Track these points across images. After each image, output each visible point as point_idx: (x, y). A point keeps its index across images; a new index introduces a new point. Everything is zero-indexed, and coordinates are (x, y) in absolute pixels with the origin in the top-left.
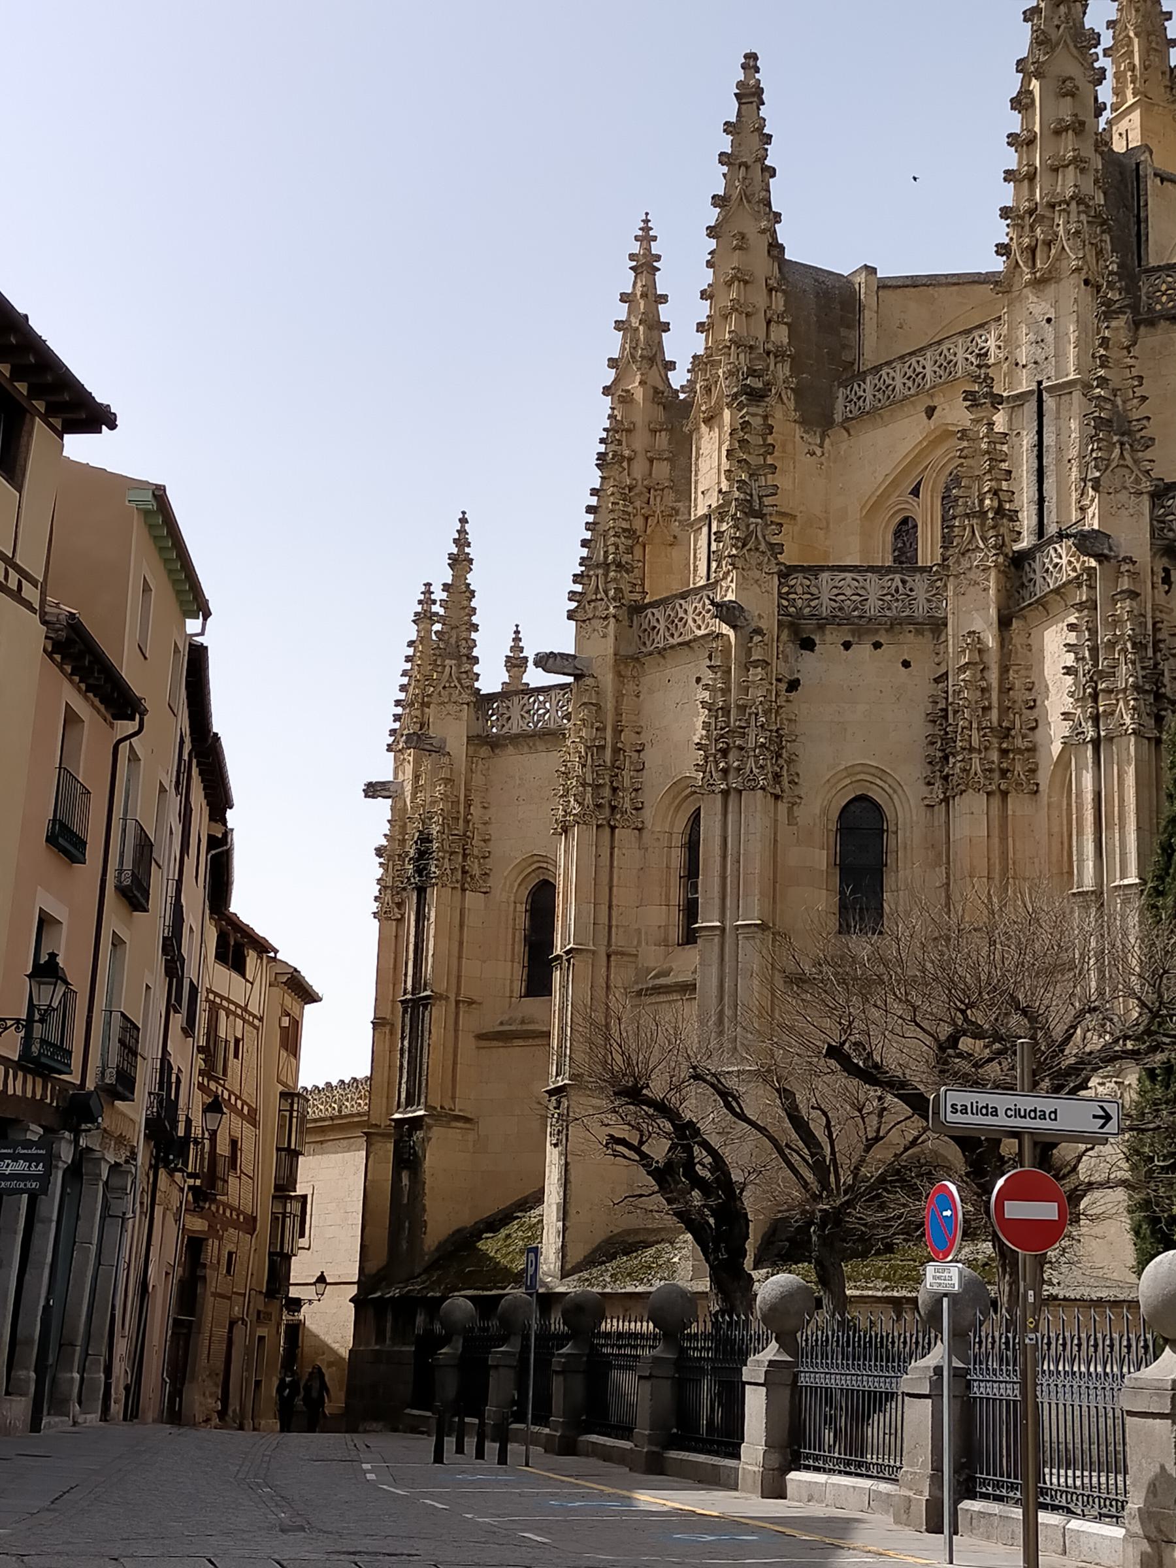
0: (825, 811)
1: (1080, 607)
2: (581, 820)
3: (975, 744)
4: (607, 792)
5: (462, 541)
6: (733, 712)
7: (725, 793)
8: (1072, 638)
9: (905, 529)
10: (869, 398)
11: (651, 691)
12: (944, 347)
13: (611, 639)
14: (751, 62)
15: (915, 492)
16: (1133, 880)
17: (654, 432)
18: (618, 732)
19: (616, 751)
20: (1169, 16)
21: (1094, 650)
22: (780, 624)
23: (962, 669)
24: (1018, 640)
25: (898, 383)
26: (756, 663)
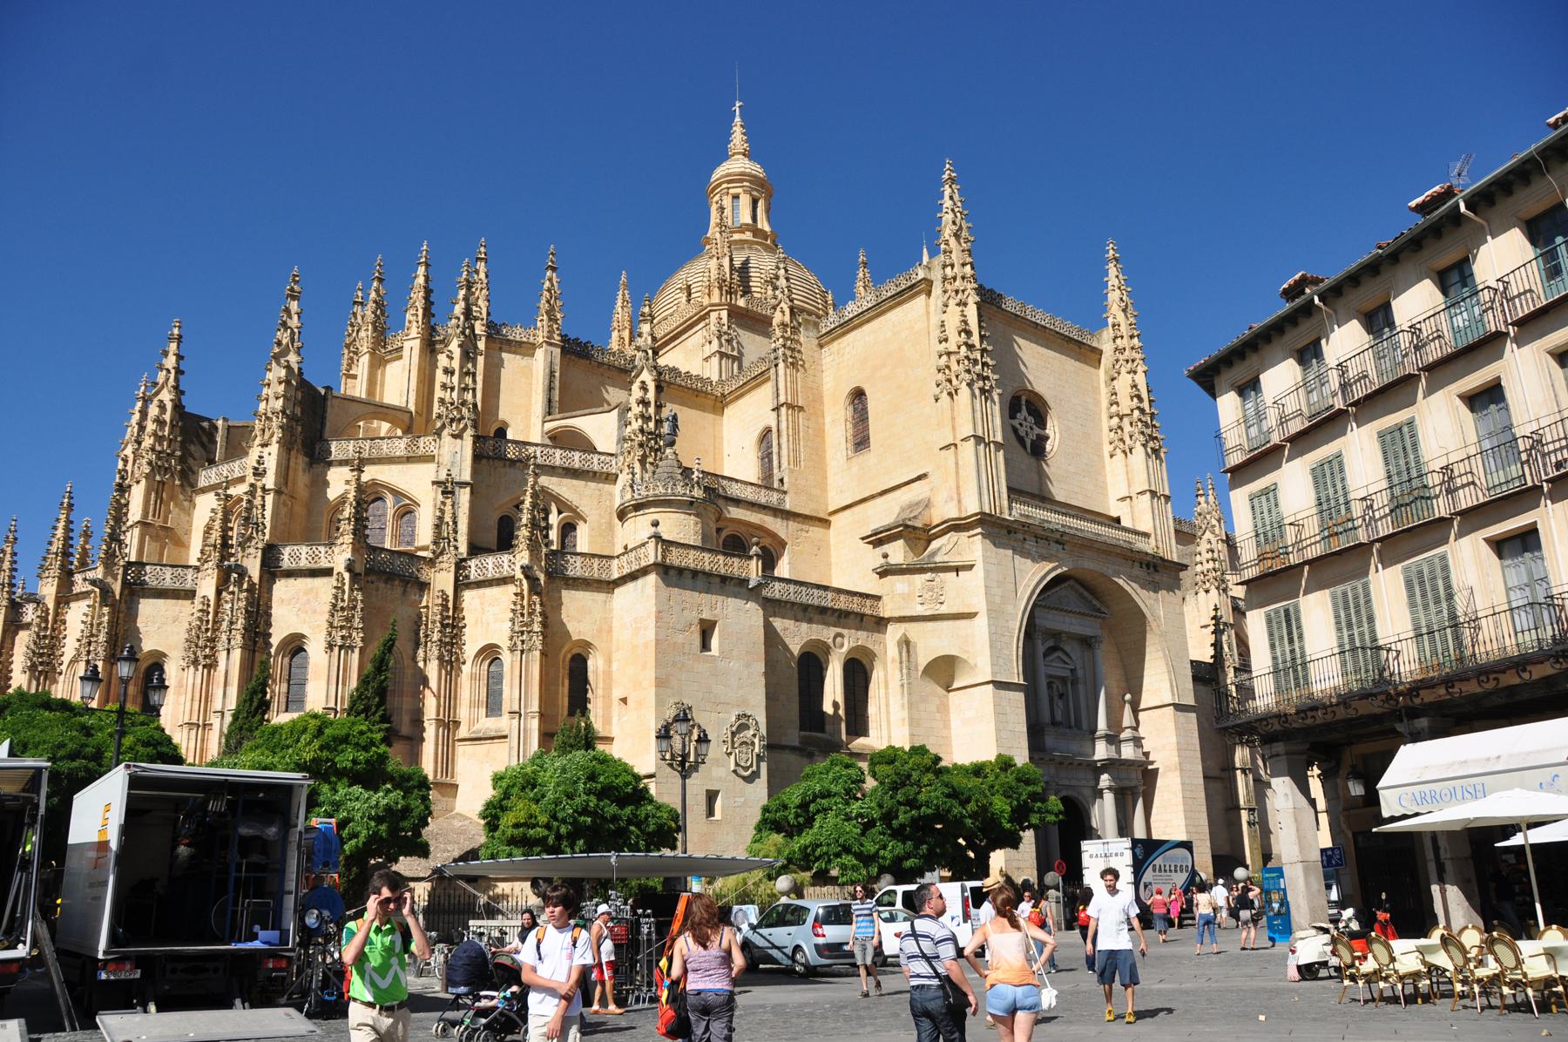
3: (201, 643)
12: (243, 460)
13: (55, 588)
21: (232, 611)
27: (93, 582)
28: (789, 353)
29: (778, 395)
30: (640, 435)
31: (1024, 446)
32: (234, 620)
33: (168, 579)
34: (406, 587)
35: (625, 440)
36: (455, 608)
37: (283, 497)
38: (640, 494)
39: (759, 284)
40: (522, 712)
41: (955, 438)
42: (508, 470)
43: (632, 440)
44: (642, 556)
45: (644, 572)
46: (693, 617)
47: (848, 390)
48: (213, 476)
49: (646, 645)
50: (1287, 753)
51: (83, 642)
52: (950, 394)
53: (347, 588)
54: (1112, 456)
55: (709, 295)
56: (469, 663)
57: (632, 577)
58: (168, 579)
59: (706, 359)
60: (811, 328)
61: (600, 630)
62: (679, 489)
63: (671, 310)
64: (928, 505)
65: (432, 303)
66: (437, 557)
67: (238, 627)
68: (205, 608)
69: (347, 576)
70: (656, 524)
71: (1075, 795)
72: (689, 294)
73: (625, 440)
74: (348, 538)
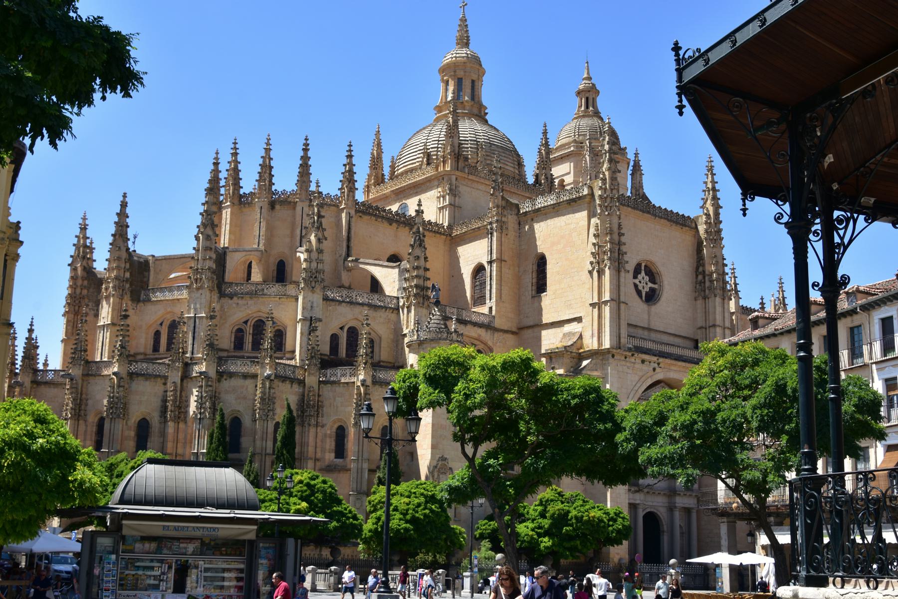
0: (135, 421)
2: (70, 418)
4: (77, 411)
5: (31, 325)
7: (111, 419)
9: (157, 334)
13: (81, 371)
14: (125, 196)
15: (161, 324)
16: (205, 451)
18: (81, 394)
19: (81, 400)
20: (241, 179)
23: (171, 391)
24: (185, 385)
26: (121, 386)
27: (114, 374)
31: (641, 297)
34: (292, 384)
41: (599, 299)
42: (338, 307)
50: (728, 522)
52: (598, 272)
54: (696, 299)
56: (326, 428)
59: (441, 209)
62: (445, 335)
64: (581, 337)
65: (273, 176)
71: (655, 511)
73: (404, 288)
74: (267, 361)
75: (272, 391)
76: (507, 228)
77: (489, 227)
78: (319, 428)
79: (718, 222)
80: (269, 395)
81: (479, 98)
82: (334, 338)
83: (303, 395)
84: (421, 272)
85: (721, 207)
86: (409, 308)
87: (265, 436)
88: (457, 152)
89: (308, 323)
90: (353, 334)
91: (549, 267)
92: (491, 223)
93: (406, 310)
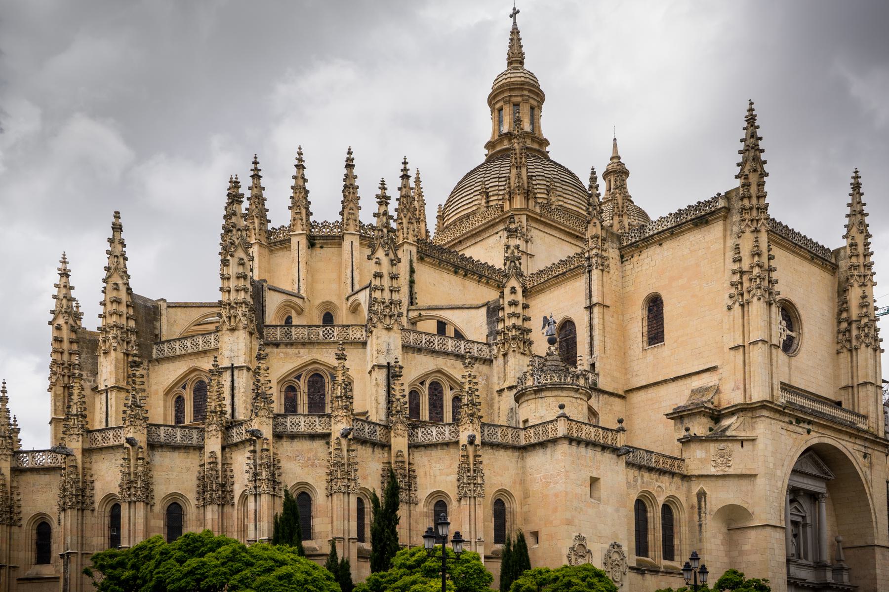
1: (251, 452)
6: (132, 475)
7: (130, 503)
8: (249, 461)
10: (166, 351)
11: (96, 462)
12: (195, 338)
15: (184, 388)
17: (71, 342)
18: (84, 476)
21: (255, 466)
22: (148, 444)
23: (210, 463)
24: (228, 455)
25: (177, 347)
26: (140, 459)
28: (599, 261)
29: (591, 296)
30: (514, 330)
32: (258, 471)
33: (179, 438)
35: (498, 333)
36: (409, 464)
37: (251, 373)
38: (539, 383)
39: (546, 192)
40: (473, 541)
41: (744, 341)
43: (505, 334)
44: (550, 430)
45: (555, 441)
46: (586, 475)
47: (646, 294)
48: (166, 349)
49: (556, 495)
51: (125, 487)
52: (742, 306)
53: (345, 448)
55: (510, 200)
56: (421, 505)
57: (542, 445)
58: (179, 438)
60: (615, 240)
61: (515, 483)
62: (569, 380)
63: (470, 210)
66: (395, 425)
67: (264, 478)
68: (214, 460)
69: (344, 442)
70: (562, 407)
72: (488, 197)
73: (498, 333)
75: (353, 454)
76: (608, 266)
77: (586, 264)
78: (412, 506)
79: (867, 255)
80: (349, 459)
81: (540, 130)
82: (414, 395)
83: (389, 463)
84: (519, 310)
85: (871, 236)
86: (505, 355)
87: (346, 512)
88: (526, 188)
89: (385, 371)
90: (436, 390)
91: (667, 310)
92: (589, 259)
93: (501, 360)
